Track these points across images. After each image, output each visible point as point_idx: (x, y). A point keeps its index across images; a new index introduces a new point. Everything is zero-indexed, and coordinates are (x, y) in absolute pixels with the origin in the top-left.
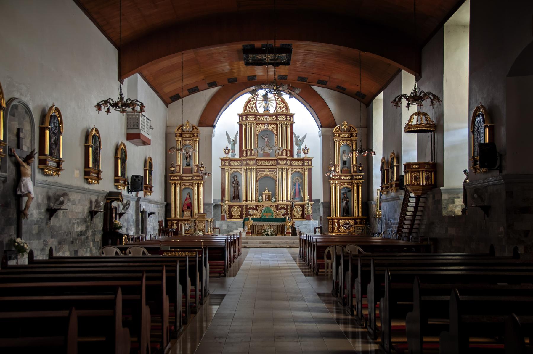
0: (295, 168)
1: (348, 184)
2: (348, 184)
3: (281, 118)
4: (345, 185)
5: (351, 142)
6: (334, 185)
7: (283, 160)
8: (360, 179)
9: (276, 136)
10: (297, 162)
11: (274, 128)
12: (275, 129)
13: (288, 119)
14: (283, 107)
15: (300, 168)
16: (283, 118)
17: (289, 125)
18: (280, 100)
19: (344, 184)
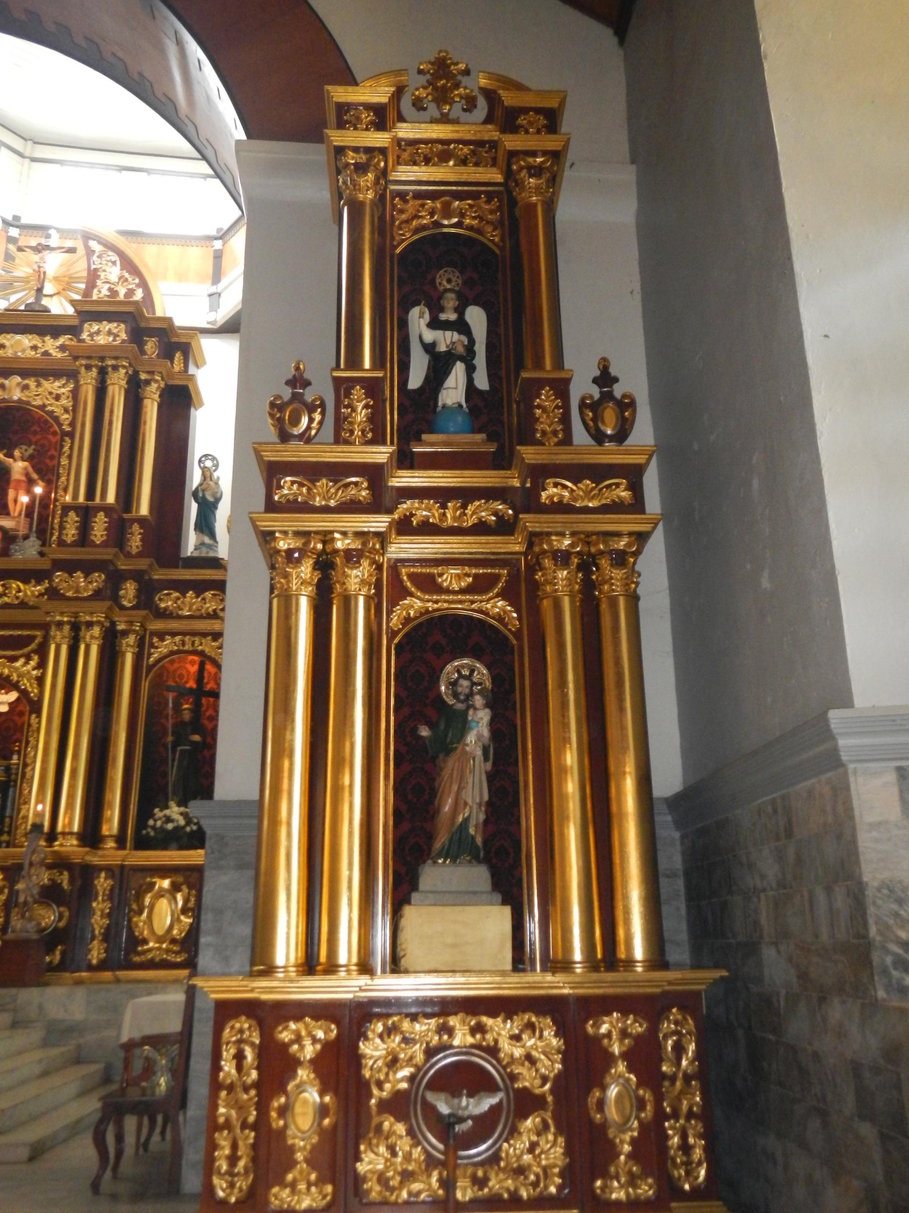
0: (173, 634)
1: (480, 586)
2: (480, 586)
3: (98, 332)
4: (440, 590)
5: (500, 208)
6: (306, 570)
7: (88, 568)
8: (615, 508)
9: (67, 439)
10: (190, 593)
11: (58, 398)
12: (66, 402)
13: (151, 346)
14: (130, 292)
15: (204, 635)
16: (110, 333)
17: (154, 386)
18: (115, 258)
19: (428, 584)
